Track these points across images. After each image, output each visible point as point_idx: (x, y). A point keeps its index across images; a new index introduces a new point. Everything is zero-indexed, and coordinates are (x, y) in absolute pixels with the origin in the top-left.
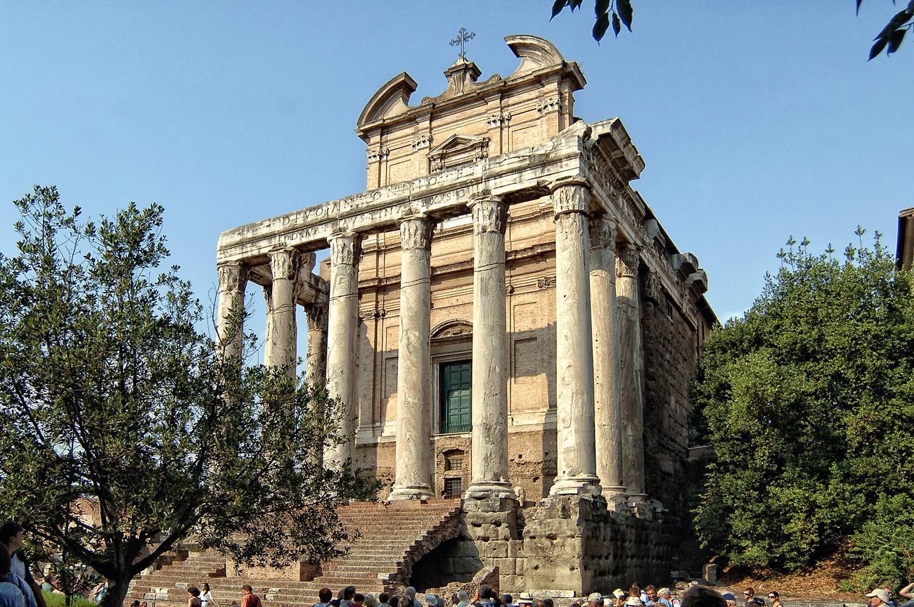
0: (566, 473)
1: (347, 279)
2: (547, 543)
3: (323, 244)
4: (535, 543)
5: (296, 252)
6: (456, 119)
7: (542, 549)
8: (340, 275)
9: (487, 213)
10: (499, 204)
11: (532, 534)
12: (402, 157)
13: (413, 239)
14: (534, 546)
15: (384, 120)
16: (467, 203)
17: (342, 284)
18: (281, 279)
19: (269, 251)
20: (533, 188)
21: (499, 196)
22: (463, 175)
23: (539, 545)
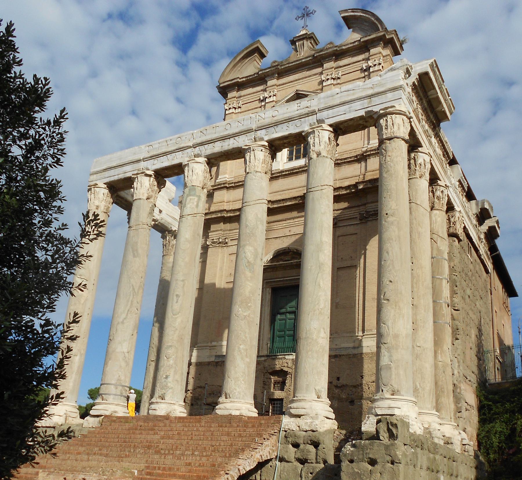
1: (196, 200)
3: (178, 170)
6: (297, 78)
8: (190, 195)
12: (252, 109)
14: (351, 471)
21: (330, 126)
22: (301, 107)
23: (356, 470)
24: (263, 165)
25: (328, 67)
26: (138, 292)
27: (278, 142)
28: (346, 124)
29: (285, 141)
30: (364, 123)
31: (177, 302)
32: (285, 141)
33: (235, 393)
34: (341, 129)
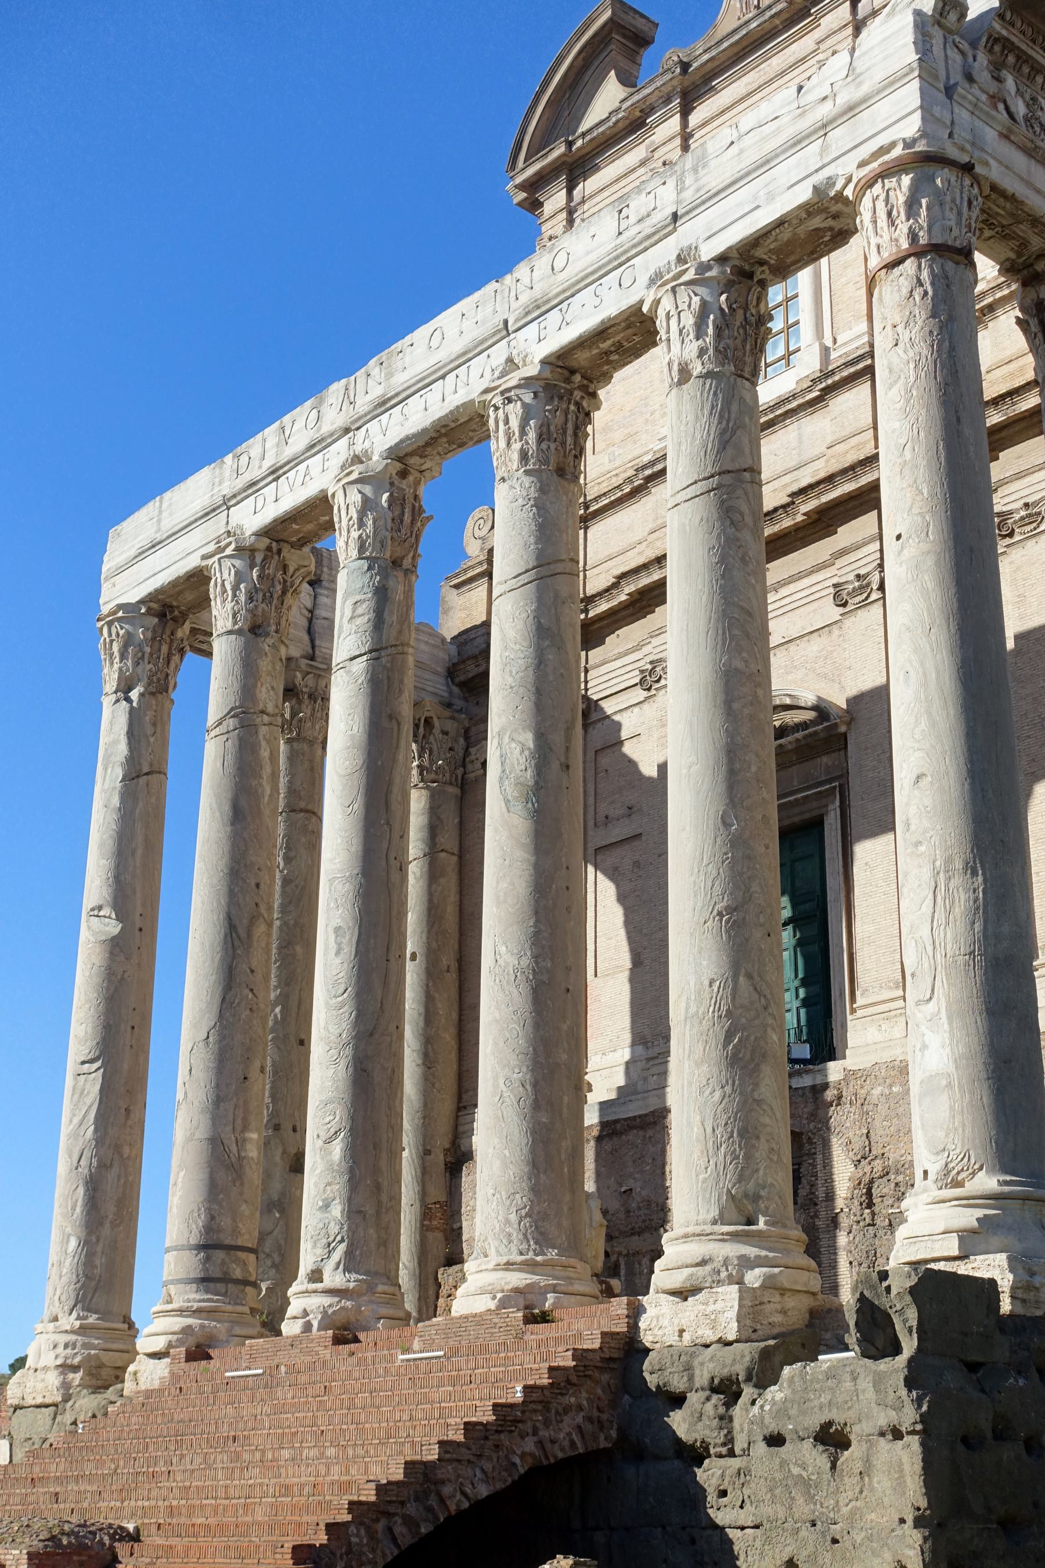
0: (931, 1176)
2: (816, 1458)
4: (783, 1463)
5: (269, 549)
6: (744, 92)
7: (806, 1485)
9: (689, 320)
10: (728, 286)
11: (773, 1427)
13: (517, 446)
14: (778, 1476)
15: (570, 144)
16: (641, 302)
17: (359, 621)
18: (230, 632)
19: (205, 557)
20: (808, 210)
21: (722, 259)
22: (633, 219)
23: (796, 1471)
24: (544, 446)
25: (835, 26)
26: (249, 935)
27: (583, 357)
28: (770, 244)
29: (605, 345)
30: (830, 222)
31: (337, 953)
32: (605, 345)
33: (510, 1235)
34: (762, 263)
